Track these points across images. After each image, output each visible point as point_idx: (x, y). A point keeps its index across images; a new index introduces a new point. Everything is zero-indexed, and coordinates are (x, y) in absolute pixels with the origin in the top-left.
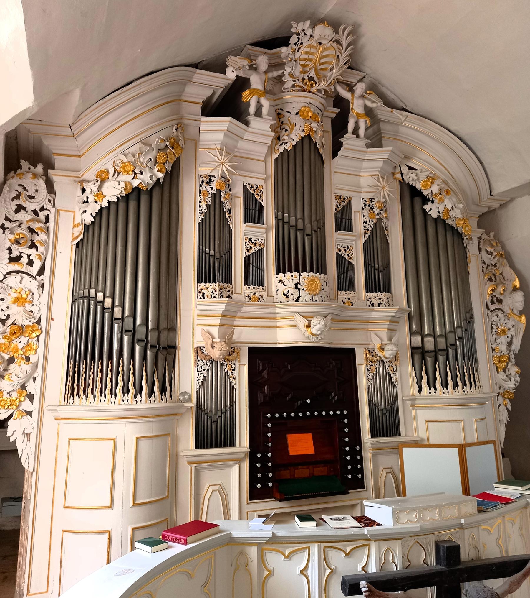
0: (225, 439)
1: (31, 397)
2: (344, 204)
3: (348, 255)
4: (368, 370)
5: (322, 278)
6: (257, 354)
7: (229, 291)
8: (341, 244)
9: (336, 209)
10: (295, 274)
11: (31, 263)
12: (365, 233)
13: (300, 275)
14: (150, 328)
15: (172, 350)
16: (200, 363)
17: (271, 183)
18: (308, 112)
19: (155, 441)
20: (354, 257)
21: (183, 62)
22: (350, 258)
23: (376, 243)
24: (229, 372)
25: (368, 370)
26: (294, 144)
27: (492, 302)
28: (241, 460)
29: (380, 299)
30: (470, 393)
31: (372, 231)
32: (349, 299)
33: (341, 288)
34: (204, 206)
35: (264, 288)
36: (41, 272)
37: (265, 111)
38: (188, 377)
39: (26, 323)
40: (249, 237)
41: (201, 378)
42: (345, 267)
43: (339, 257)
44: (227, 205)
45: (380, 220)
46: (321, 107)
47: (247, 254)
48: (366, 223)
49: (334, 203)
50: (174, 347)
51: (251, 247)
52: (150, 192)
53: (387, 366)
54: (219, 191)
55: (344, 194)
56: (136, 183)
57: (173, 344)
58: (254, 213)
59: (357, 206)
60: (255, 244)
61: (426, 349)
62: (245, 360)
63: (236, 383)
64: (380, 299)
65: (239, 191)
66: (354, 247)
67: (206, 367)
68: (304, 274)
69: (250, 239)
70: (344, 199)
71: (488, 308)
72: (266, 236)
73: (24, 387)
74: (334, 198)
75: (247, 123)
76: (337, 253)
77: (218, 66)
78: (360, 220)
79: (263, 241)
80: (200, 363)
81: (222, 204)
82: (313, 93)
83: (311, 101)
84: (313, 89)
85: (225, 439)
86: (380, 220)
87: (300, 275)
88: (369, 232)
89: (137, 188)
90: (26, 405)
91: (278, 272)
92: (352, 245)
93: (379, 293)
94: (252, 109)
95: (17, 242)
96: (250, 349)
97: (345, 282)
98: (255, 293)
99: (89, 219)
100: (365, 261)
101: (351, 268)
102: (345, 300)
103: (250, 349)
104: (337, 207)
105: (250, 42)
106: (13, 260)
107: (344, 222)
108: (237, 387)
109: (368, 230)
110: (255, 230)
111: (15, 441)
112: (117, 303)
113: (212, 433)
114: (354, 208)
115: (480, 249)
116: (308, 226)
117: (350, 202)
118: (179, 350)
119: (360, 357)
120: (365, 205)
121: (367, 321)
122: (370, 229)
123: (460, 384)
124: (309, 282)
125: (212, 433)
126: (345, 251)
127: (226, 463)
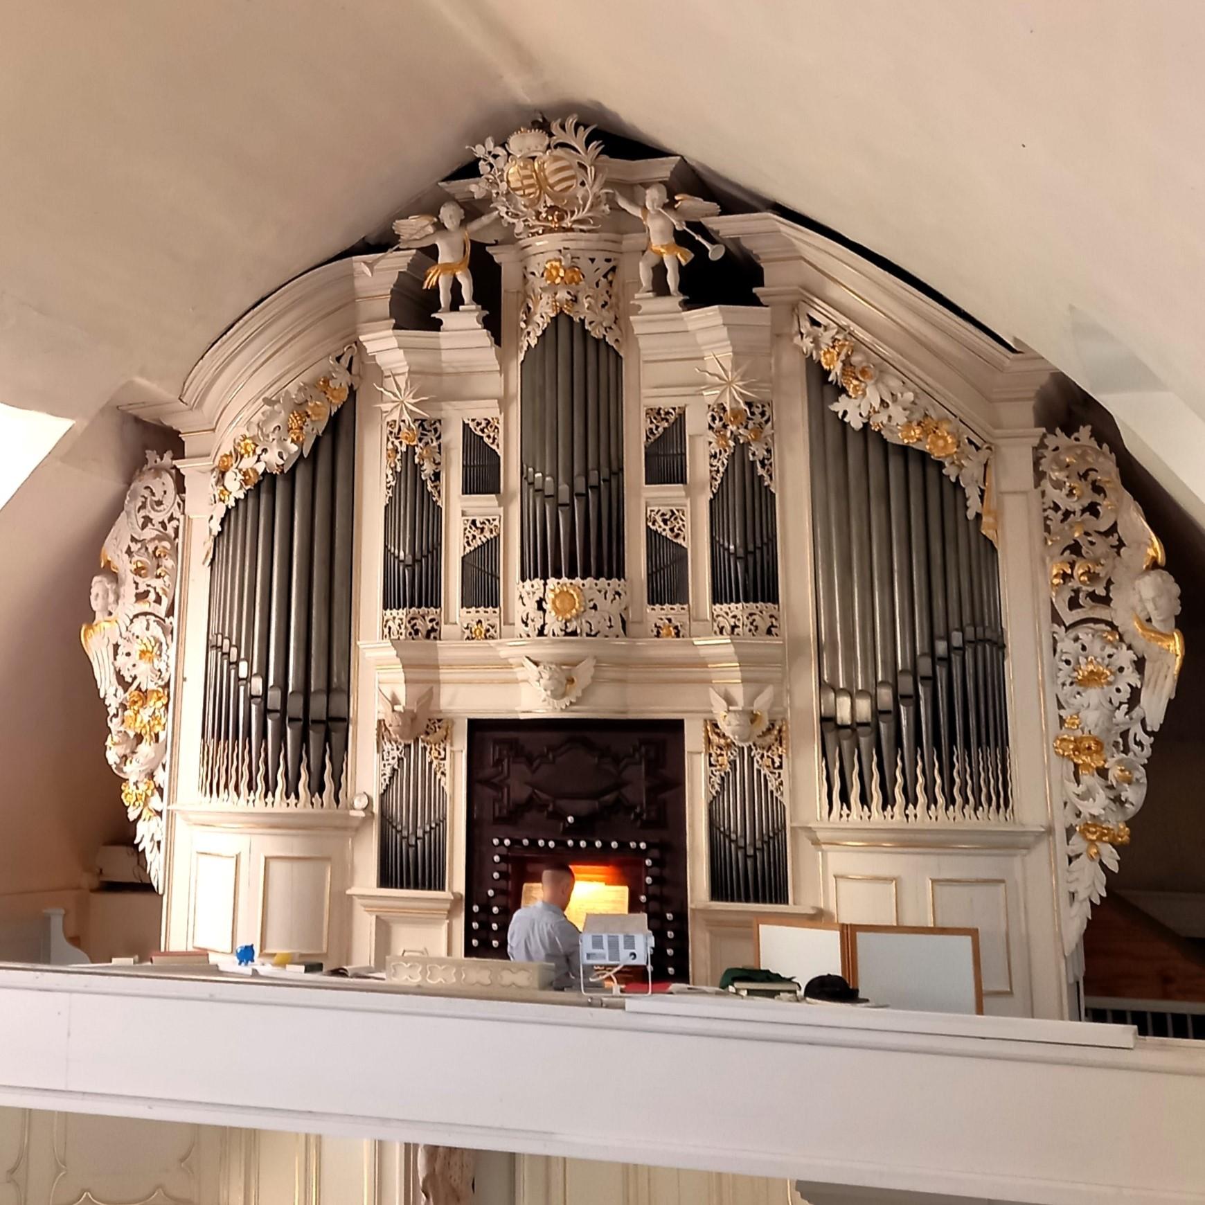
0: (431, 877)
1: (160, 790)
2: (666, 425)
3: (672, 530)
4: (711, 765)
5: (587, 586)
6: (482, 732)
7: (431, 621)
8: (656, 509)
9: (648, 437)
10: (538, 582)
12: (713, 478)
13: (545, 584)
14: (290, 690)
15: (343, 725)
16: (387, 747)
18: (557, 269)
19: (296, 865)
20: (687, 531)
21: (331, 255)
22: (677, 536)
24: (435, 762)
25: (711, 765)
26: (539, 333)
27: (1074, 604)
28: (451, 914)
29: (734, 617)
30: (987, 820)
31: (726, 470)
32: (670, 620)
33: (655, 598)
34: (391, 478)
35: (497, 610)
37: (466, 292)
38: (367, 770)
39: (152, 686)
40: (471, 518)
41: (388, 771)
42: (666, 555)
43: (652, 535)
45: (742, 448)
46: (609, 246)
47: (468, 549)
48: (714, 456)
49: (645, 425)
50: (345, 720)
51: (474, 537)
52: (291, 475)
53: (757, 758)
54: (411, 450)
55: (665, 404)
56: (260, 468)
57: (343, 715)
58: (482, 475)
59: (697, 423)
60: (482, 530)
61: (839, 722)
62: (460, 745)
63: (446, 782)
64: (734, 617)
66: (688, 510)
67: (396, 753)
68: (552, 581)
69: (474, 522)
70: (668, 413)
71: (1056, 618)
72: (505, 516)
73: (151, 776)
74: (643, 414)
75: (436, 325)
76: (648, 527)
77: (383, 242)
78: (703, 455)
79: (496, 523)
80: (387, 747)
82: (571, 230)
83: (567, 244)
84: (567, 223)
85: (431, 877)
86: (742, 448)
87: (545, 584)
88: (721, 475)
89: (265, 473)
90: (155, 803)
91: (523, 580)
93: (733, 605)
94: (444, 298)
96: (472, 723)
97: (667, 583)
98: (480, 622)
100: (712, 538)
101: (680, 556)
102: (660, 623)
103: (472, 723)
104: (652, 432)
105: (439, 178)
107: (666, 464)
108: (447, 789)
109: (718, 471)
110: (483, 505)
111: (144, 850)
112: (242, 656)
113: (408, 866)
114: (689, 430)
115: (1039, 476)
116: (564, 488)
117: (681, 417)
118: (356, 723)
119: (693, 738)
120: (714, 419)
121: (705, 665)
122: (722, 470)
123: (959, 799)
124: (556, 596)
125: (408, 866)
126: (665, 521)
127: (423, 918)
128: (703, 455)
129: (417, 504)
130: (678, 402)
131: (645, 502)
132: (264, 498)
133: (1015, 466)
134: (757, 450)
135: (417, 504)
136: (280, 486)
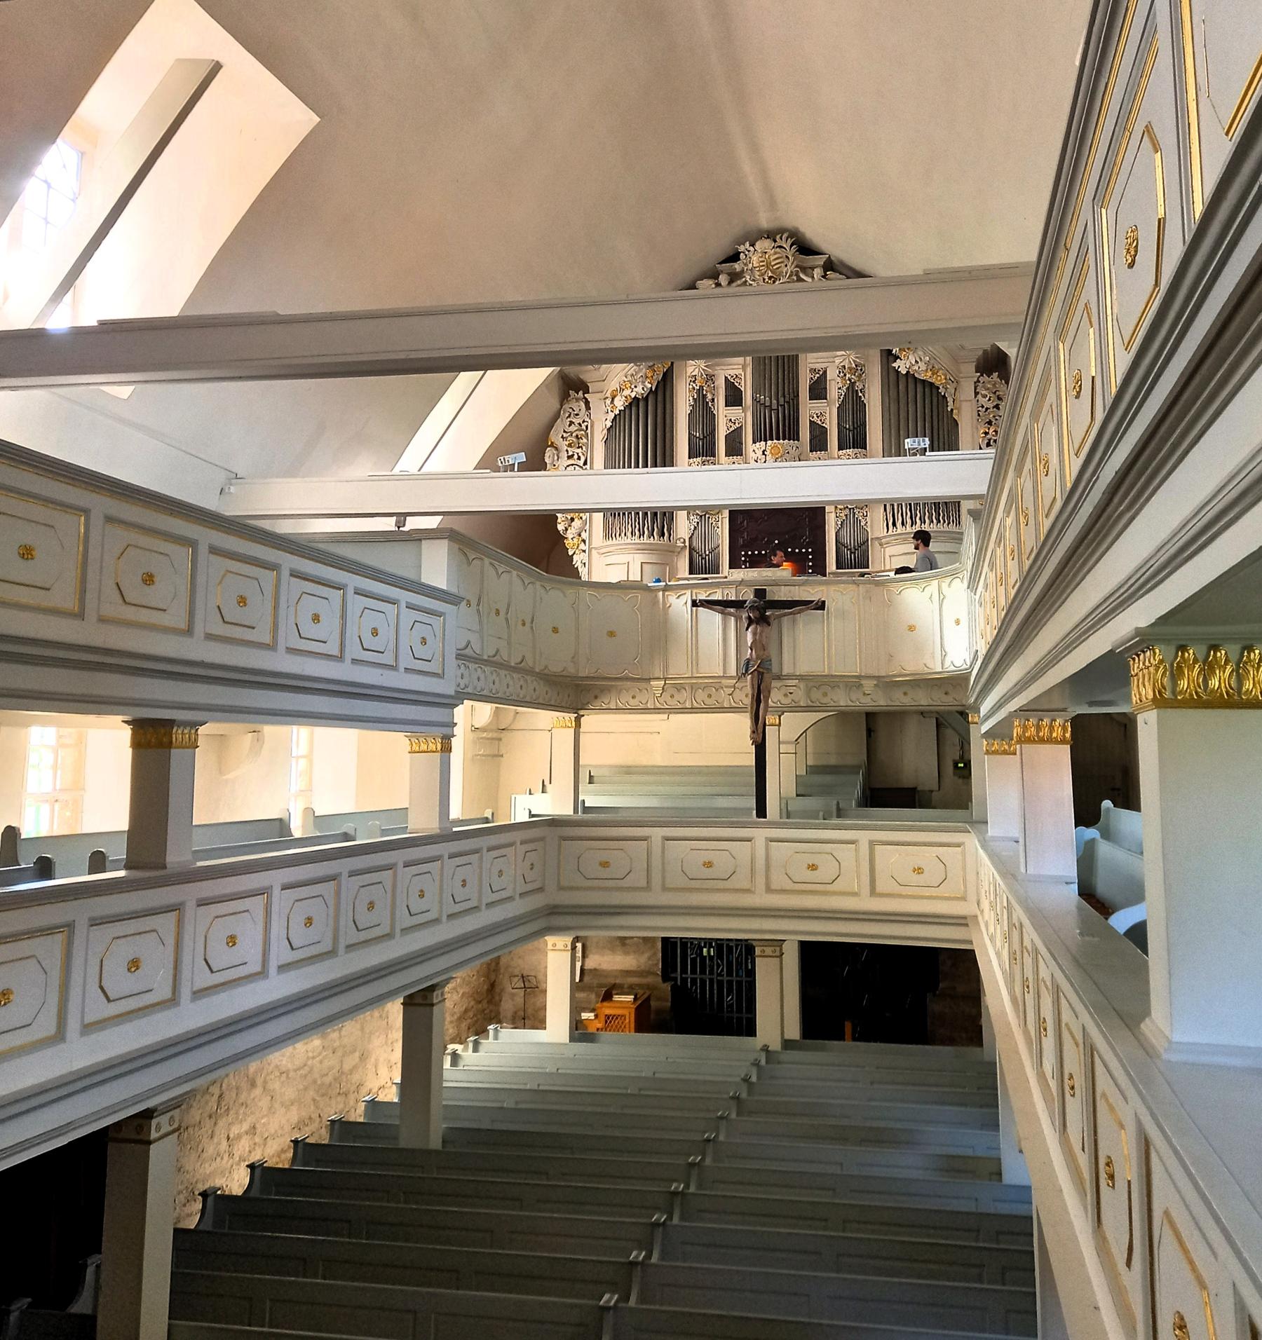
11: (579, 458)
17: (749, 370)
23: (853, 406)
36: (585, 463)
44: (709, 396)
45: (853, 384)
54: (701, 387)
55: (818, 366)
65: (721, 383)
72: (744, 416)
81: (704, 396)
86: (853, 384)
92: (828, 413)
95: (570, 445)
99: (609, 424)
106: (569, 457)
110: (735, 412)
115: (976, 394)
117: (825, 372)
128: (835, 389)
129: (703, 413)
130: (824, 366)
131: (809, 409)
132: (634, 409)
133: (967, 389)
134: (859, 386)
135: (703, 413)
136: (641, 404)
